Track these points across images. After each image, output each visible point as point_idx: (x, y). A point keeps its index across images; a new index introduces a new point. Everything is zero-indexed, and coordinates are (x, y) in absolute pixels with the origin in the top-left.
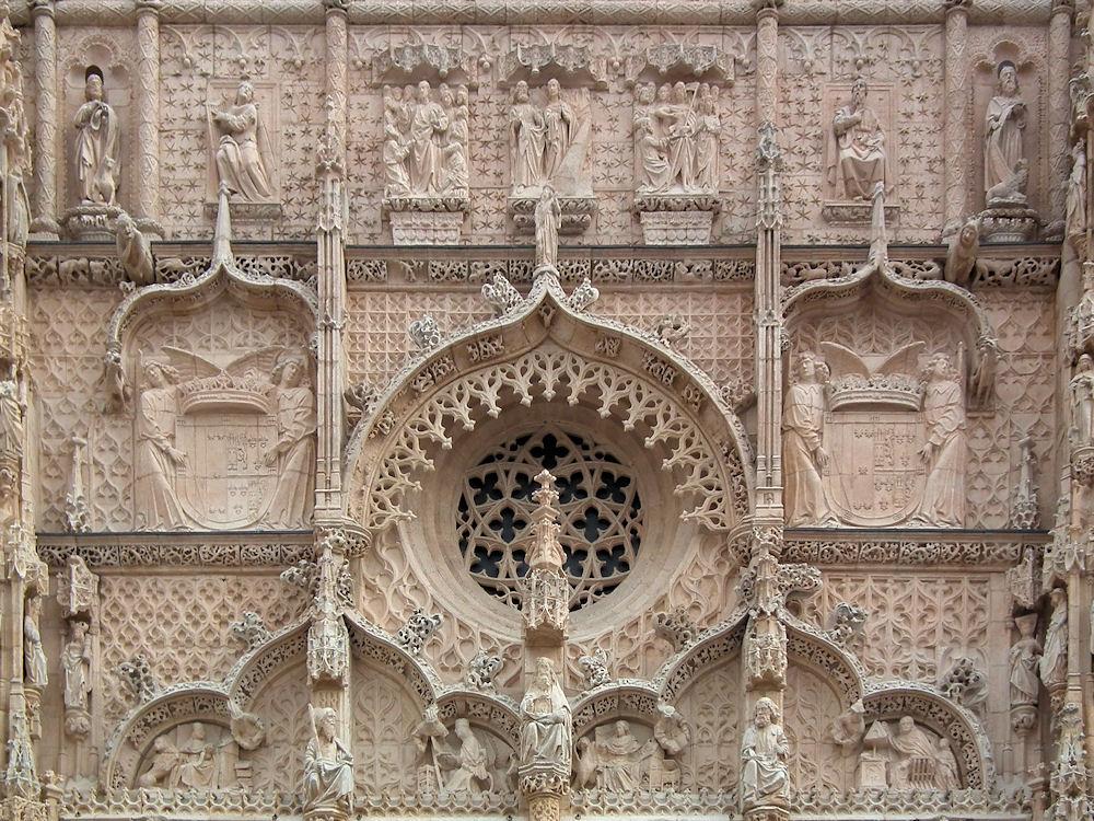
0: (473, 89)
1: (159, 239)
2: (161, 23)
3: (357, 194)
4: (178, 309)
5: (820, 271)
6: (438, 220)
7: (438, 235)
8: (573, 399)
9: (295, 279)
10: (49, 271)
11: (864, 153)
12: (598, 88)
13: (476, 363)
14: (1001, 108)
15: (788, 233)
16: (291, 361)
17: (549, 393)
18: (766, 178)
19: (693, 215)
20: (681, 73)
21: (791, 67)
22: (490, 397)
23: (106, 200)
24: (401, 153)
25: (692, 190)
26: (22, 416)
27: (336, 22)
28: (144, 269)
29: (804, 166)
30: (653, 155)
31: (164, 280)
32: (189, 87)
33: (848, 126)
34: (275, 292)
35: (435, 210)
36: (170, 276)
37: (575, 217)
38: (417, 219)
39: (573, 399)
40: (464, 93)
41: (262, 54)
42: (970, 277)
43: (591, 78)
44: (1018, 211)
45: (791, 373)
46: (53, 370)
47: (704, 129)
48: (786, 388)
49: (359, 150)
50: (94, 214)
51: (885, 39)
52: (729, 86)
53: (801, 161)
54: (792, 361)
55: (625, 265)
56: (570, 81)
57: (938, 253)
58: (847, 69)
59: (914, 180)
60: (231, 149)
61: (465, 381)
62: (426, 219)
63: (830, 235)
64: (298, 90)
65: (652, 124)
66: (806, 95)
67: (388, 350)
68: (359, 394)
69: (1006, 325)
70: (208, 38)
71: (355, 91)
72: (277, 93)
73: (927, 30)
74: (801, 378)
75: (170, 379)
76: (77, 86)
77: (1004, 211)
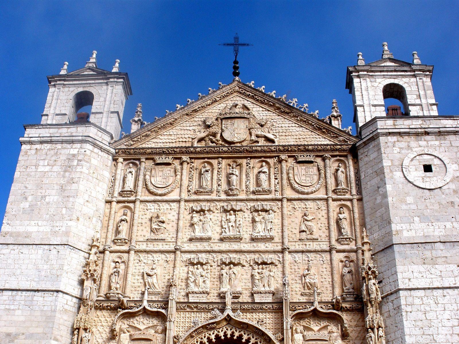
0: (211, 266)
1: (129, 299)
2: (135, 252)
3: (181, 289)
4: (132, 315)
5: (301, 307)
6: (201, 295)
7: (201, 299)
8: (235, 338)
9: (163, 309)
10: (101, 306)
11: (312, 280)
12: (243, 266)
13: (209, 329)
14: (346, 270)
15: (293, 298)
16: (160, 328)
17: (229, 336)
18: (285, 288)
19: (267, 295)
20: (264, 263)
21: (293, 261)
22: (213, 337)
23: (117, 290)
24: (192, 280)
25: (267, 289)
26: (89, 341)
27: (178, 252)
28: (125, 306)
29: (296, 283)
30: (257, 281)
31: (129, 309)
32: (140, 266)
33: (307, 275)
34: (158, 312)
35: (201, 293)
36: (131, 308)
37: (236, 295)
38: (196, 295)
39: (235, 338)
40: (209, 267)
41: (159, 259)
42: (341, 309)
43: (241, 264)
44: (352, 293)
45: (294, 331)
46: (99, 328)
47: (270, 275)
48: (292, 335)
49: (182, 279)
50: (113, 293)
51: (316, 255)
52: (276, 266)
53: (296, 282)
54: (294, 329)
55: (249, 306)
56: (235, 265)
57: (332, 303)
58: (307, 262)
59: (325, 286)
60: (150, 280)
61: (206, 333)
62: (198, 295)
63: (304, 299)
64: (167, 266)
65: (256, 274)
66: (296, 267)
67: (187, 325)
68: (177, 337)
69: (351, 319)
70: (146, 255)
71: (181, 266)
72: (162, 267)
73: (326, 254)
74: (297, 333)
75: (128, 331)
76: (113, 265)
77: (349, 293)
